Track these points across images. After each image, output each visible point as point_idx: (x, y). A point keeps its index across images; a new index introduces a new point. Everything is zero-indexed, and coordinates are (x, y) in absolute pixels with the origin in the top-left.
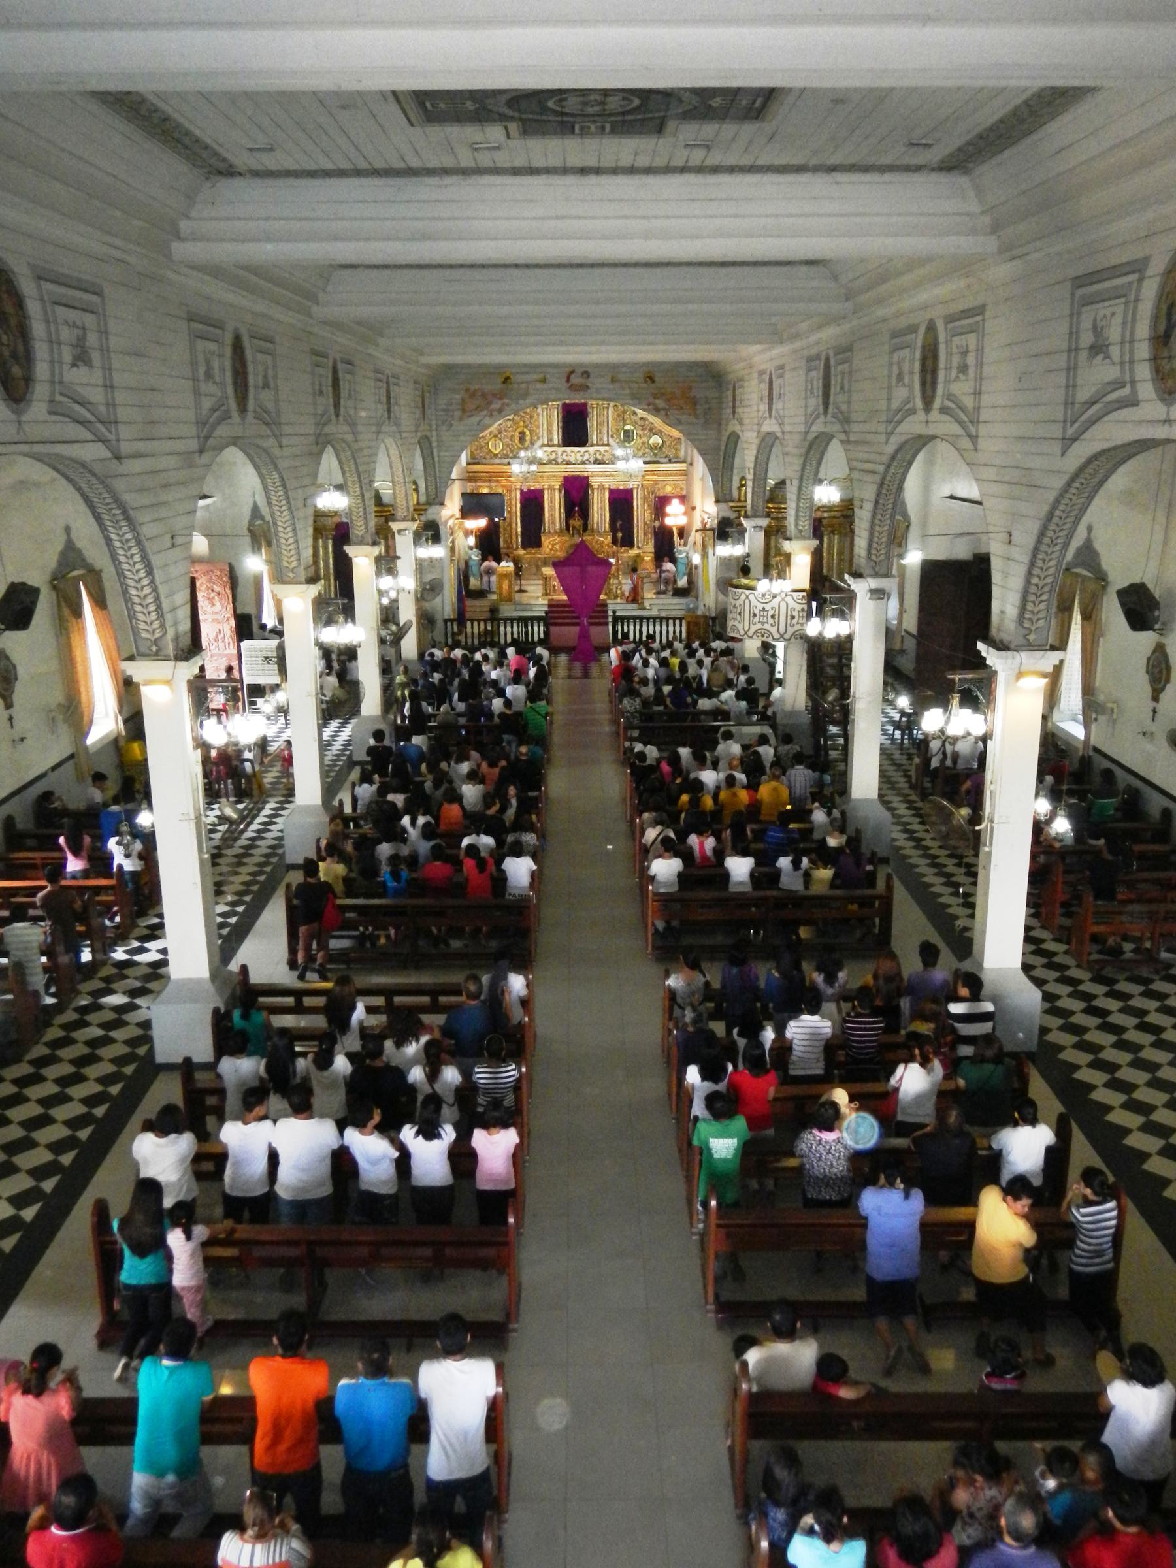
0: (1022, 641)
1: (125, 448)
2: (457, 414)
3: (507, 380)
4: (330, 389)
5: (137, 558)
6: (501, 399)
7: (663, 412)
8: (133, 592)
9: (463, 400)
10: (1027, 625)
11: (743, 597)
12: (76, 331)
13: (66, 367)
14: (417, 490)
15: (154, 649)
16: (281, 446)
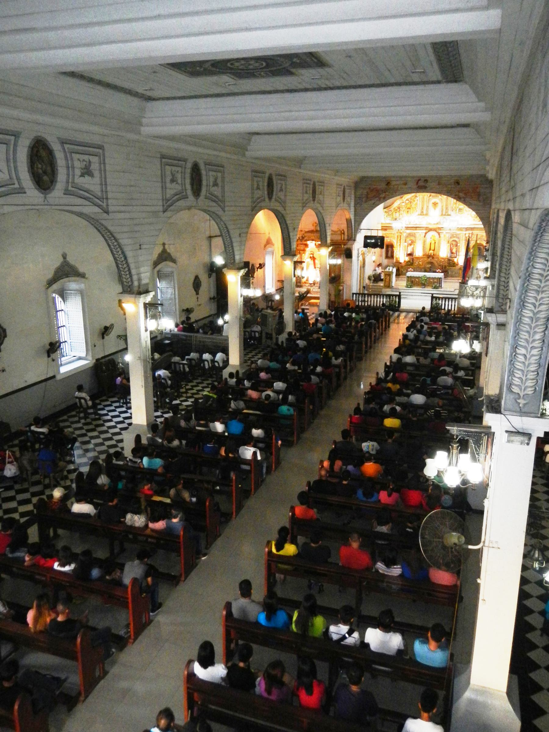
0: (500, 309)
1: (111, 209)
2: (364, 199)
3: (388, 184)
4: (266, 188)
5: (120, 253)
6: (385, 192)
7: (463, 199)
8: (120, 266)
9: (367, 192)
10: (501, 301)
11: (464, 288)
12: (85, 163)
13: (76, 177)
14: (344, 234)
15: (129, 289)
16: (224, 211)
